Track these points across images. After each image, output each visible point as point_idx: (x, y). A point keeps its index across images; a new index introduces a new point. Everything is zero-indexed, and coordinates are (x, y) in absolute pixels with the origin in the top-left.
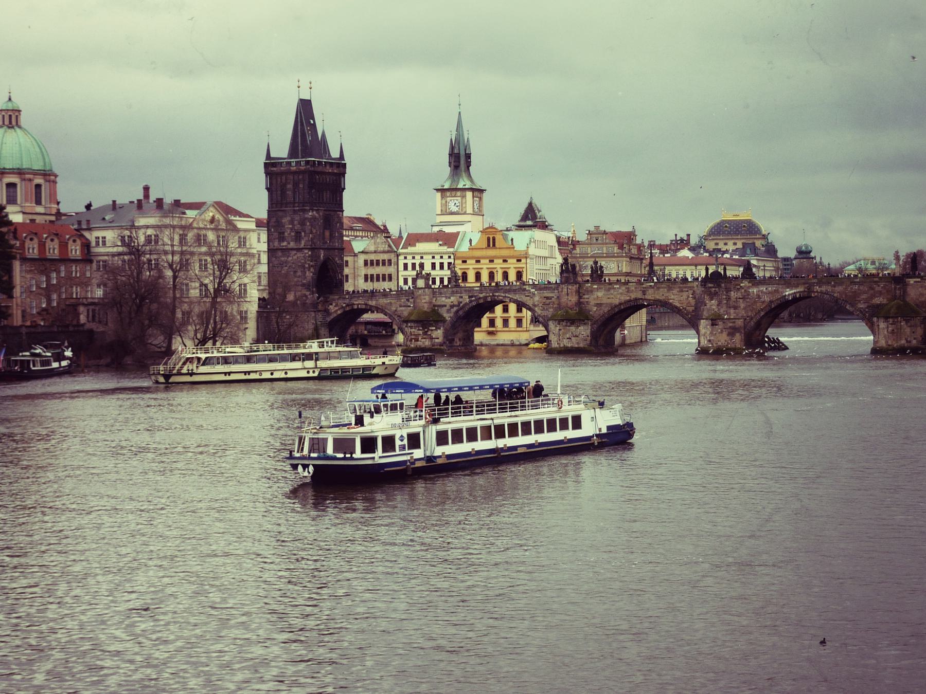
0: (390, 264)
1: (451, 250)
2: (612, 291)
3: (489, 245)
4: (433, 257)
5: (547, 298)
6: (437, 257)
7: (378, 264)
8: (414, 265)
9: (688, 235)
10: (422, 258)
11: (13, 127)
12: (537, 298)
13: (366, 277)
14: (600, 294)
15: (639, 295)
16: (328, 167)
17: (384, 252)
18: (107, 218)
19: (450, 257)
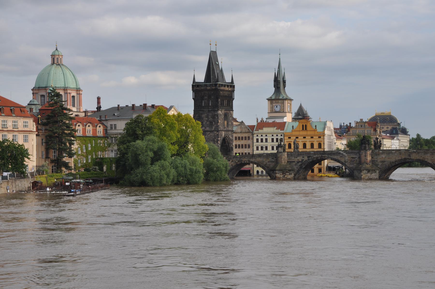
0: (249, 139)
1: (282, 131)
2: (391, 154)
3: (303, 129)
4: (273, 136)
5: (353, 158)
6: (275, 135)
7: (242, 139)
8: (277, 139)
9: (350, 123)
10: (266, 136)
11: (59, 65)
12: (347, 158)
13: (236, 145)
14: (384, 156)
15: (407, 157)
16: (226, 87)
17: (246, 132)
18: (116, 114)
19: (281, 135)
